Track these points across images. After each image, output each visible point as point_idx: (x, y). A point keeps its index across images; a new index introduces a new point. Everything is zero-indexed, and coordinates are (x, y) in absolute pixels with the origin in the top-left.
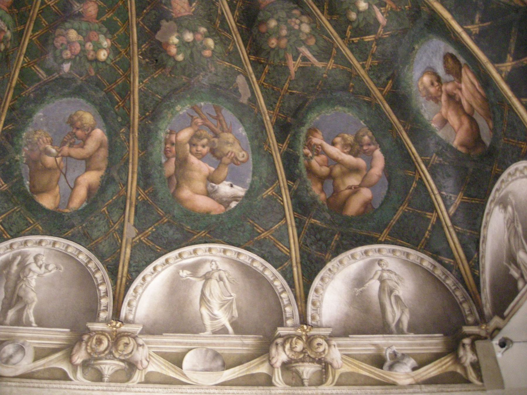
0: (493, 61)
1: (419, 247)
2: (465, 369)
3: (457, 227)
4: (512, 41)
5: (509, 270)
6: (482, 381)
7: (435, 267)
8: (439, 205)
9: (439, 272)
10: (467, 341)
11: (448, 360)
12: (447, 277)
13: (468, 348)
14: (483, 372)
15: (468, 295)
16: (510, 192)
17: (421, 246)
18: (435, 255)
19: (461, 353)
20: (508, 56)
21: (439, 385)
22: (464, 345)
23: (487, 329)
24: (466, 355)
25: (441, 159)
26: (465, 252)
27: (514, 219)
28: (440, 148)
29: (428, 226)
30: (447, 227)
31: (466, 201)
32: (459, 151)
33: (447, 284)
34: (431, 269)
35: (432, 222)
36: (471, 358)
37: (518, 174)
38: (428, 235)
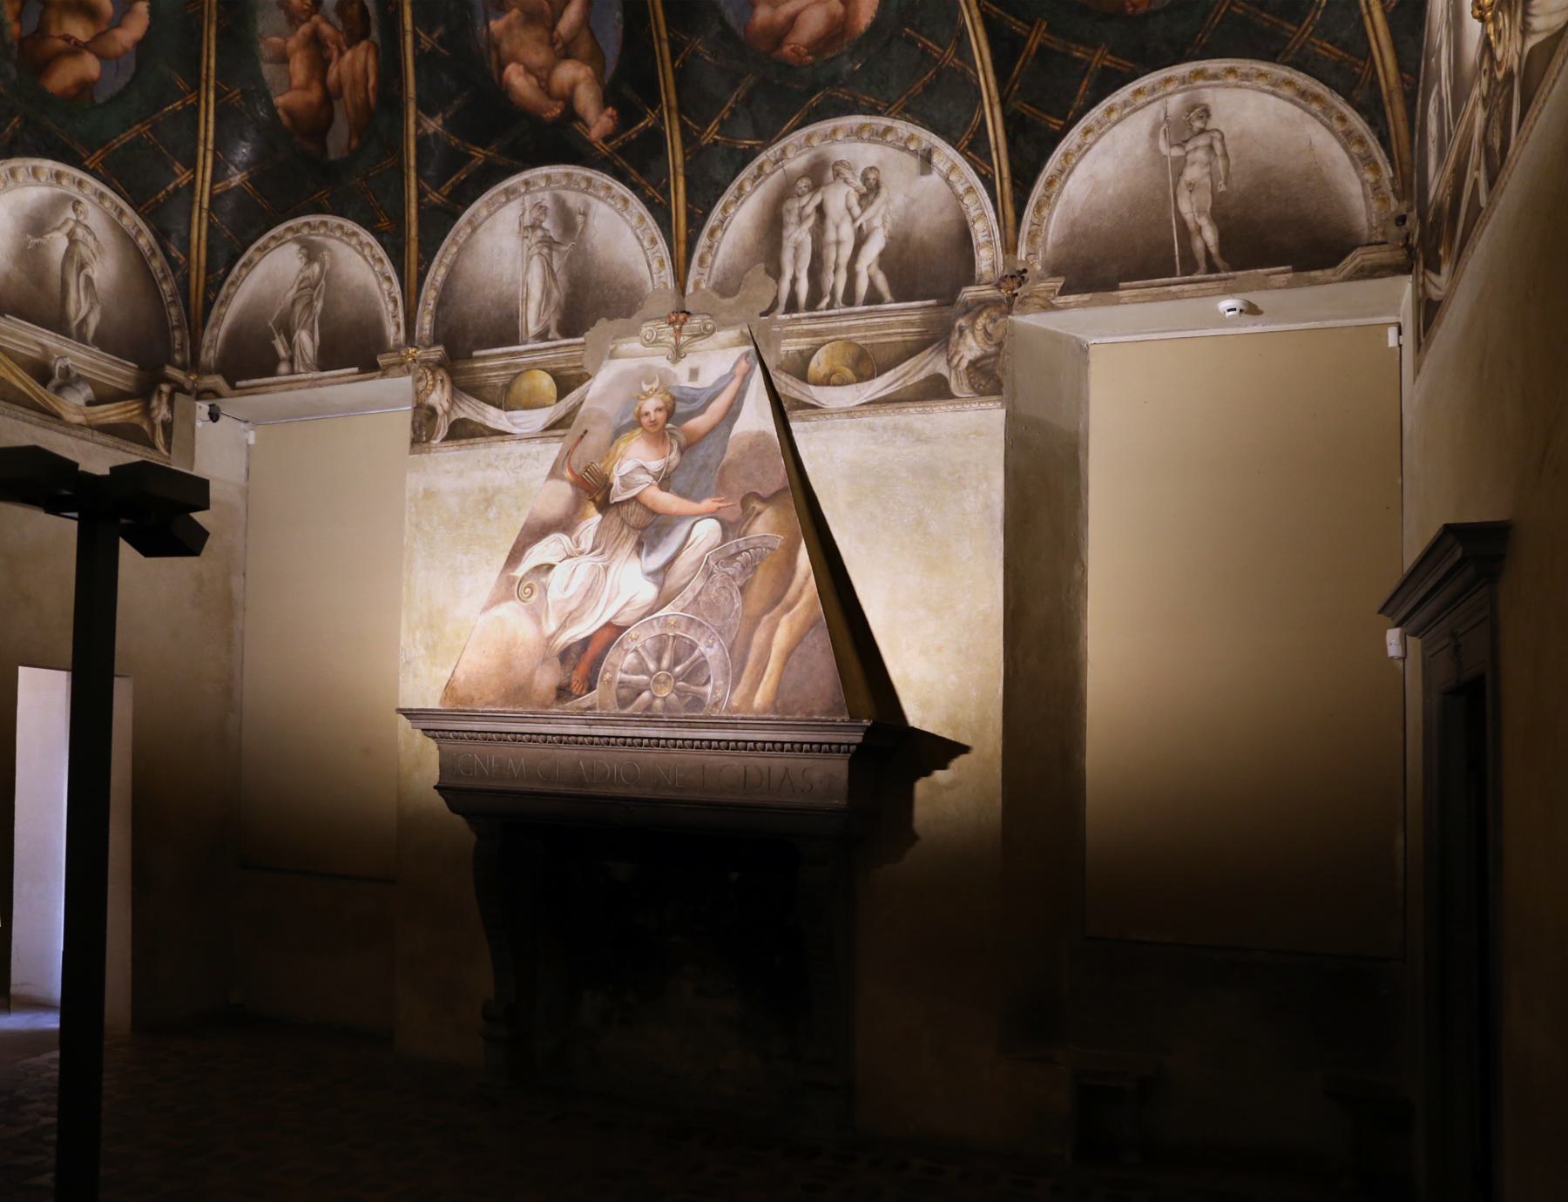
0: (421, 105)
1: (142, 209)
2: (153, 426)
3: (213, 216)
4: (456, 102)
5: (274, 339)
6: (169, 451)
7: (154, 253)
8: (204, 167)
9: (156, 264)
10: (165, 388)
11: (135, 406)
12: (165, 278)
13: (165, 399)
14: (174, 441)
15: (185, 319)
16: (330, 250)
17: (144, 210)
18: (161, 235)
19: (155, 403)
20: (440, 115)
21: (117, 439)
22: (160, 392)
23: (197, 383)
24: (159, 407)
25: (243, 104)
26: (208, 259)
27: (317, 286)
28: (253, 88)
29: (169, 184)
30: (201, 208)
31: (248, 191)
32: (277, 115)
33: (163, 289)
34: (149, 254)
35: (178, 181)
36: (165, 415)
37: (354, 241)
38: (163, 196)
